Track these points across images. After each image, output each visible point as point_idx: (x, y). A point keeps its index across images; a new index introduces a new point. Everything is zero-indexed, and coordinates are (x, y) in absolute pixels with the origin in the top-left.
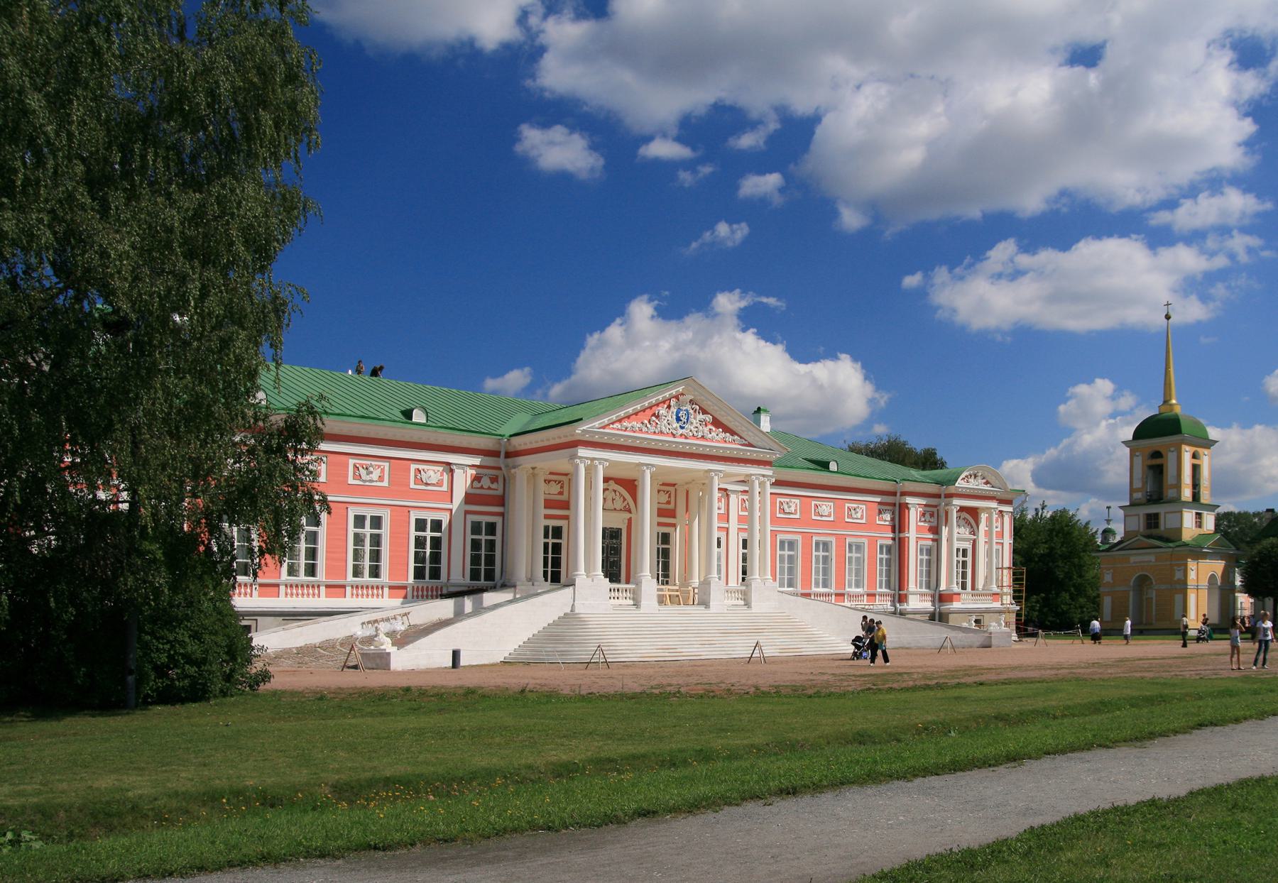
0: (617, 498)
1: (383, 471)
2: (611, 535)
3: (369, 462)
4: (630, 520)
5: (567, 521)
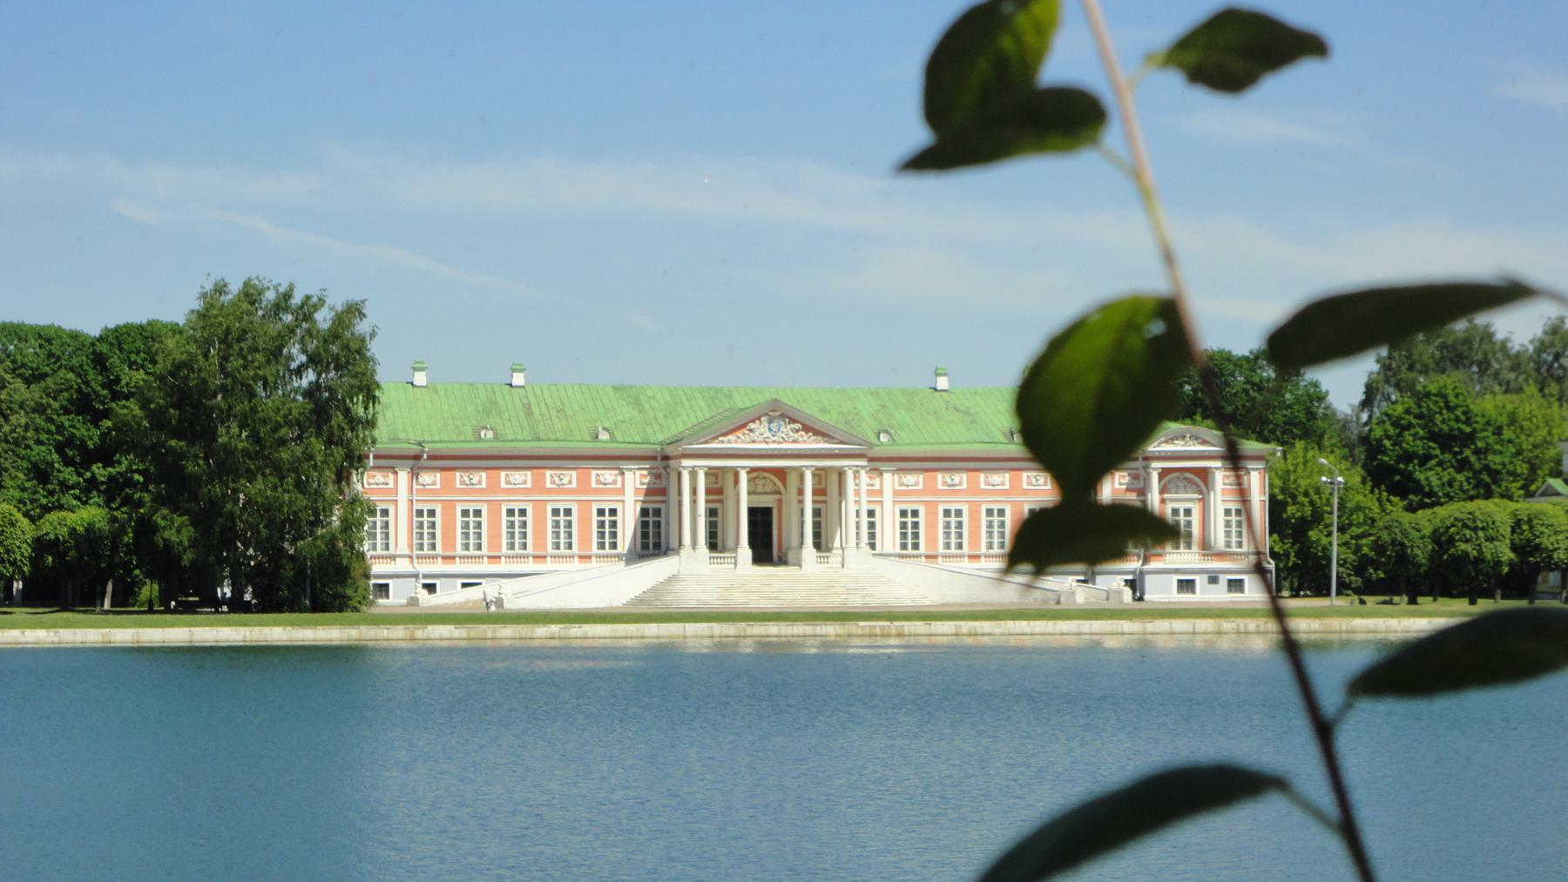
0: (768, 483)
1: (571, 477)
2: (857, 512)
3: (559, 472)
4: (780, 501)
5: (721, 504)
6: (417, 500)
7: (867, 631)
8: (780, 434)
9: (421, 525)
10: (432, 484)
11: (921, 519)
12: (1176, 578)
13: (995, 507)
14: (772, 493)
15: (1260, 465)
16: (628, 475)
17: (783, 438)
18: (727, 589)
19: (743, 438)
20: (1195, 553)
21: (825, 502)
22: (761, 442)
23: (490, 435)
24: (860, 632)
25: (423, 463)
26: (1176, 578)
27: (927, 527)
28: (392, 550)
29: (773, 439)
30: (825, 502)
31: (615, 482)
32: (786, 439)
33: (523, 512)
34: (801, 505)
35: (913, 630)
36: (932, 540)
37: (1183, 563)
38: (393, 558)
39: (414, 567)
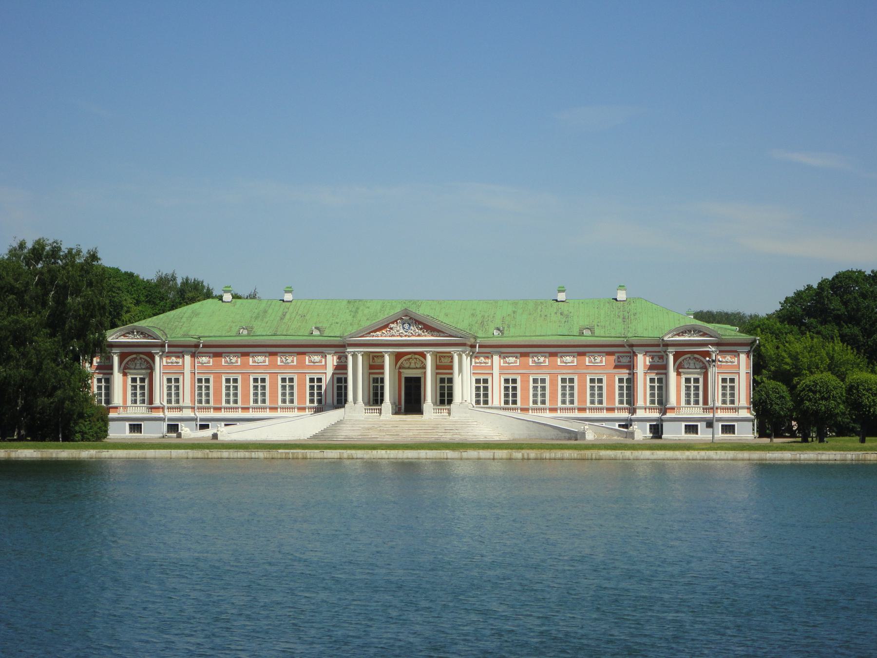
6: (198, 373)
7: (284, 456)
8: (410, 331)
9: (200, 388)
10: (207, 363)
11: (518, 385)
12: (683, 424)
13: (568, 377)
14: (420, 368)
15: (747, 349)
16: (329, 357)
17: (411, 333)
18: (369, 429)
19: (386, 333)
20: (700, 407)
22: (397, 336)
23: (245, 332)
24: (279, 456)
25: (201, 349)
26: (683, 424)
27: (521, 390)
28: (181, 404)
29: (406, 334)
31: (320, 362)
32: (414, 334)
33: (263, 380)
35: (312, 455)
36: (525, 399)
37: (688, 414)
38: (180, 409)
39: (195, 414)
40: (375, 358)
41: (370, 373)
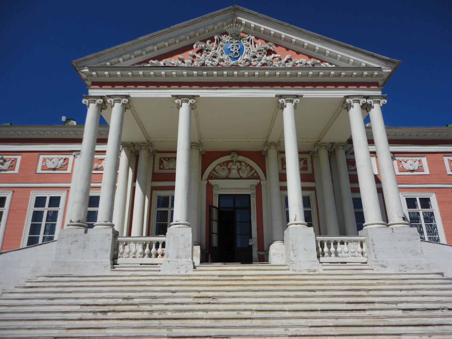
0: (243, 168)
4: (259, 187)
14: (248, 178)
21: (313, 189)
30: (313, 189)
34: (284, 192)
40: (164, 162)
41: (154, 189)
